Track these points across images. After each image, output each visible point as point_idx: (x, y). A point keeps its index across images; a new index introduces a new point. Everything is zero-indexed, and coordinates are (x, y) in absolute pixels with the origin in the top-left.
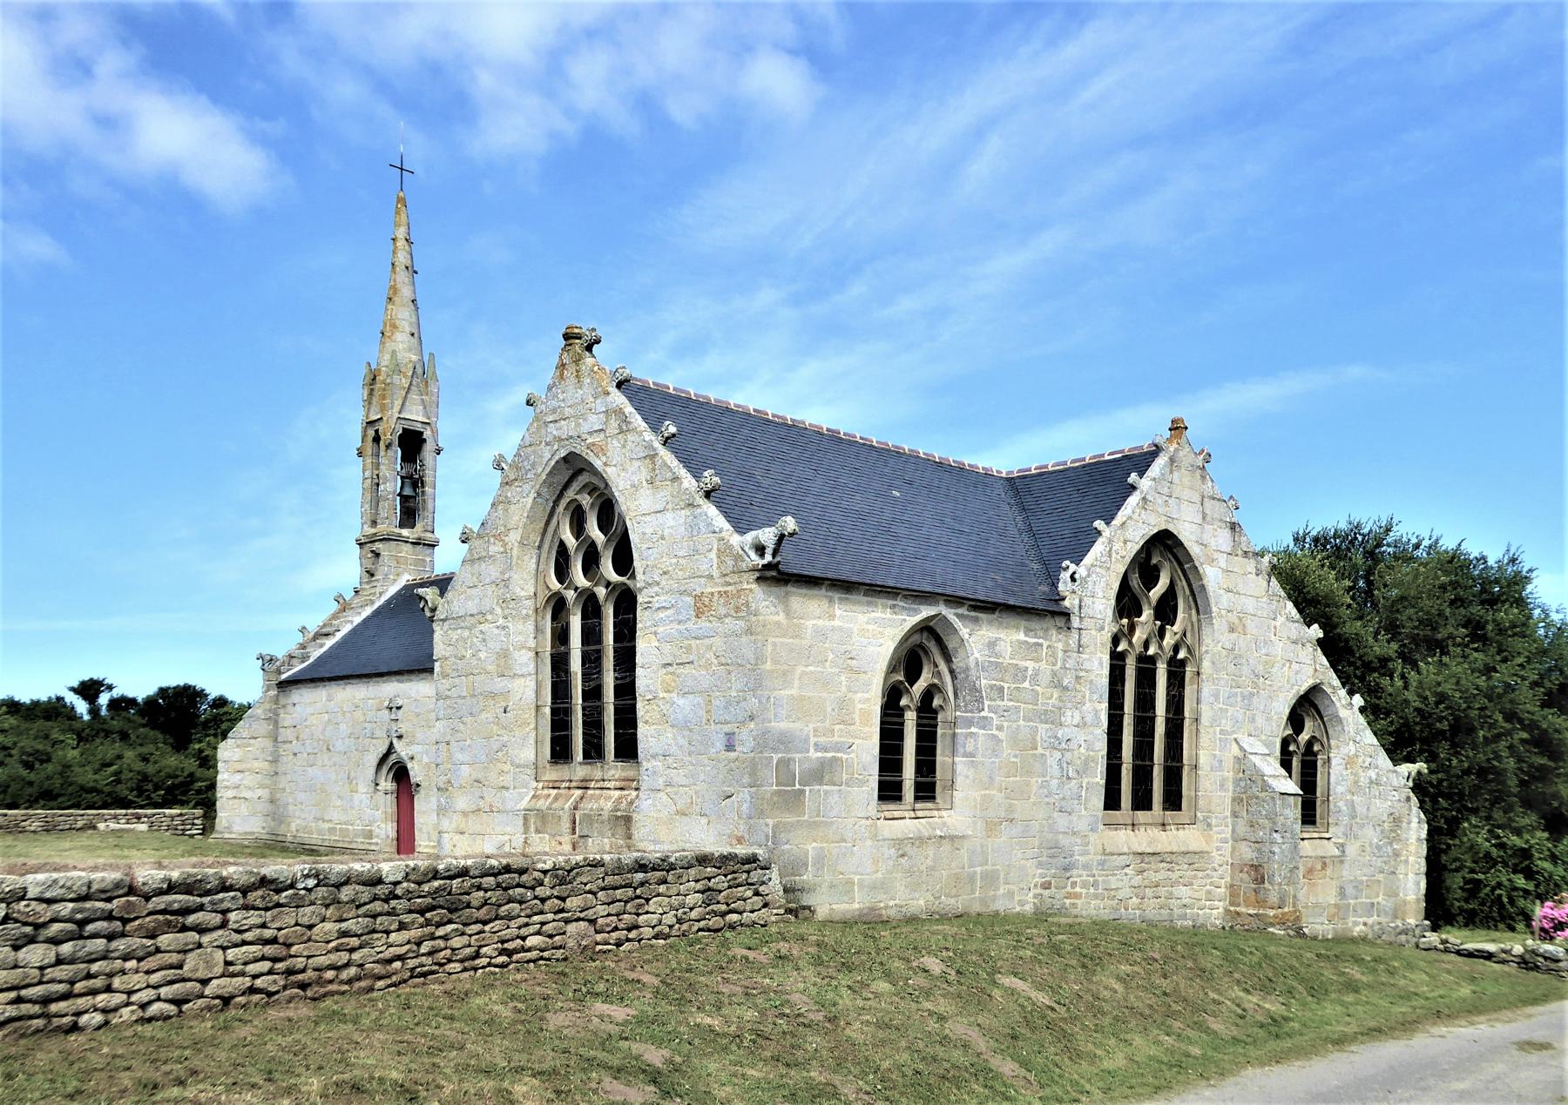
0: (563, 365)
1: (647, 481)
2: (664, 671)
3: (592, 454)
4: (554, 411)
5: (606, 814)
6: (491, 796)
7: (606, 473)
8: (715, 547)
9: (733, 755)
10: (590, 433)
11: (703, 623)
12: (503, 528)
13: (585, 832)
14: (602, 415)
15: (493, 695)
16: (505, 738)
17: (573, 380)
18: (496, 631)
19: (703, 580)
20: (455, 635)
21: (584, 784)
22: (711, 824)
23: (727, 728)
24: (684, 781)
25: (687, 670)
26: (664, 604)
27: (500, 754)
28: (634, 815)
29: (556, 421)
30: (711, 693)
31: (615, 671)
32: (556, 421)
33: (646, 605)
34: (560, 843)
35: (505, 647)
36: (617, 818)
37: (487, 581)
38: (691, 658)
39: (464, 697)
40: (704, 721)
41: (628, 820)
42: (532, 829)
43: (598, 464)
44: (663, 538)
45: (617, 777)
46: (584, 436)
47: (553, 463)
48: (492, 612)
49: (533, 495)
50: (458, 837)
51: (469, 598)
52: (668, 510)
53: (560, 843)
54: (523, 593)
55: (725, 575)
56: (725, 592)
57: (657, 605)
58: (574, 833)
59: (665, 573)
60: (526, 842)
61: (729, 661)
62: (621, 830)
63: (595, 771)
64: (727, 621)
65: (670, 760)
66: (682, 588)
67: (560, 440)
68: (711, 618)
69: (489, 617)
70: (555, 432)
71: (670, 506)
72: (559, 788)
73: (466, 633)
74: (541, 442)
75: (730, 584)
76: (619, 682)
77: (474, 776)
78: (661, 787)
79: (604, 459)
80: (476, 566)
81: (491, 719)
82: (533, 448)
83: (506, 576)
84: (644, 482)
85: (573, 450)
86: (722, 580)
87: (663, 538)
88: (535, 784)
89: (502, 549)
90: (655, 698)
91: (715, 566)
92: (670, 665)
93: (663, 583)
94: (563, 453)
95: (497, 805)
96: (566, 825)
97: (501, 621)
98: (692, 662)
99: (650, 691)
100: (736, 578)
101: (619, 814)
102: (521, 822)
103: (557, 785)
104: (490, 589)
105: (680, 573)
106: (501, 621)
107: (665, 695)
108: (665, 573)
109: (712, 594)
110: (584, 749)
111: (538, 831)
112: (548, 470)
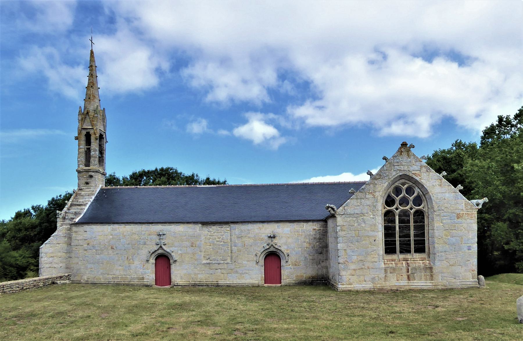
0: (402, 151)
1: (438, 185)
2: (445, 231)
3: (414, 176)
4: (398, 162)
5: (422, 267)
6: (367, 265)
7: (421, 181)
8: (464, 203)
9: (470, 251)
10: (414, 170)
11: (459, 220)
12: (373, 191)
13: (414, 272)
14: (419, 166)
15: (369, 237)
16: (375, 248)
17: (406, 155)
18: (370, 219)
19: (460, 210)
20: (349, 219)
21: (406, 260)
22: (463, 268)
23: (468, 245)
24: (453, 258)
25: (454, 231)
26: (445, 215)
27: (372, 253)
28: (433, 267)
29: (398, 165)
30: (462, 237)
31: (414, 230)
32: (398, 165)
33: (438, 215)
34: (402, 276)
35: (374, 223)
36: (426, 268)
37: (365, 205)
38: (455, 228)
39: (354, 237)
40: (460, 243)
41: (431, 268)
42: (389, 272)
43: (417, 178)
44: (445, 199)
45: (417, 257)
46: (411, 171)
47: (396, 176)
48: (368, 213)
49: (387, 183)
50: (351, 276)
51: (355, 209)
52: (447, 193)
53: (402, 276)
54: (380, 209)
55: (467, 210)
56: (467, 213)
57: (443, 215)
58: (408, 272)
59: (446, 208)
60: (385, 276)
61: (469, 229)
62: (428, 271)
63: (408, 256)
64: (468, 220)
65: (447, 253)
66: (453, 212)
67: (400, 170)
68: (463, 219)
69: (367, 215)
70: (398, 168)
71: (447, 192)
72: (395, 261)
73: (355, 219)
74: (391, 170)
75: (469, 212)
76: (415, 233)
77: (360, 259)
78: (444, 259)
79: (420, 178)
80: (359, 201)
81: (368, 243)
82: (388, 171)
83: (375, 204)
84: (437, 185)
85: (405, 173)
86: (466, 211)
87: (445, 199)
88: (383, 261)
89: (373, 197)
90: (442, 238)
91: (464, 207)
92: (447, 230)
93: (445, 210)
94: (401, 174)
95: (371, 265)
96: (404, 270)
97: (372, 216)
98: (455, 229)
99: (440, 236)
100: (471, 210)
101: (427, 267)
102: (383, 271)
103: (394, 260)
104: (366, 207)
105: (452, 208)
106: (372, 216)
107: (445, 237)
108: (446, 208)
109: (463, 214)
110: (400, 251)
111: (391, 273)
112: (394, 177)
